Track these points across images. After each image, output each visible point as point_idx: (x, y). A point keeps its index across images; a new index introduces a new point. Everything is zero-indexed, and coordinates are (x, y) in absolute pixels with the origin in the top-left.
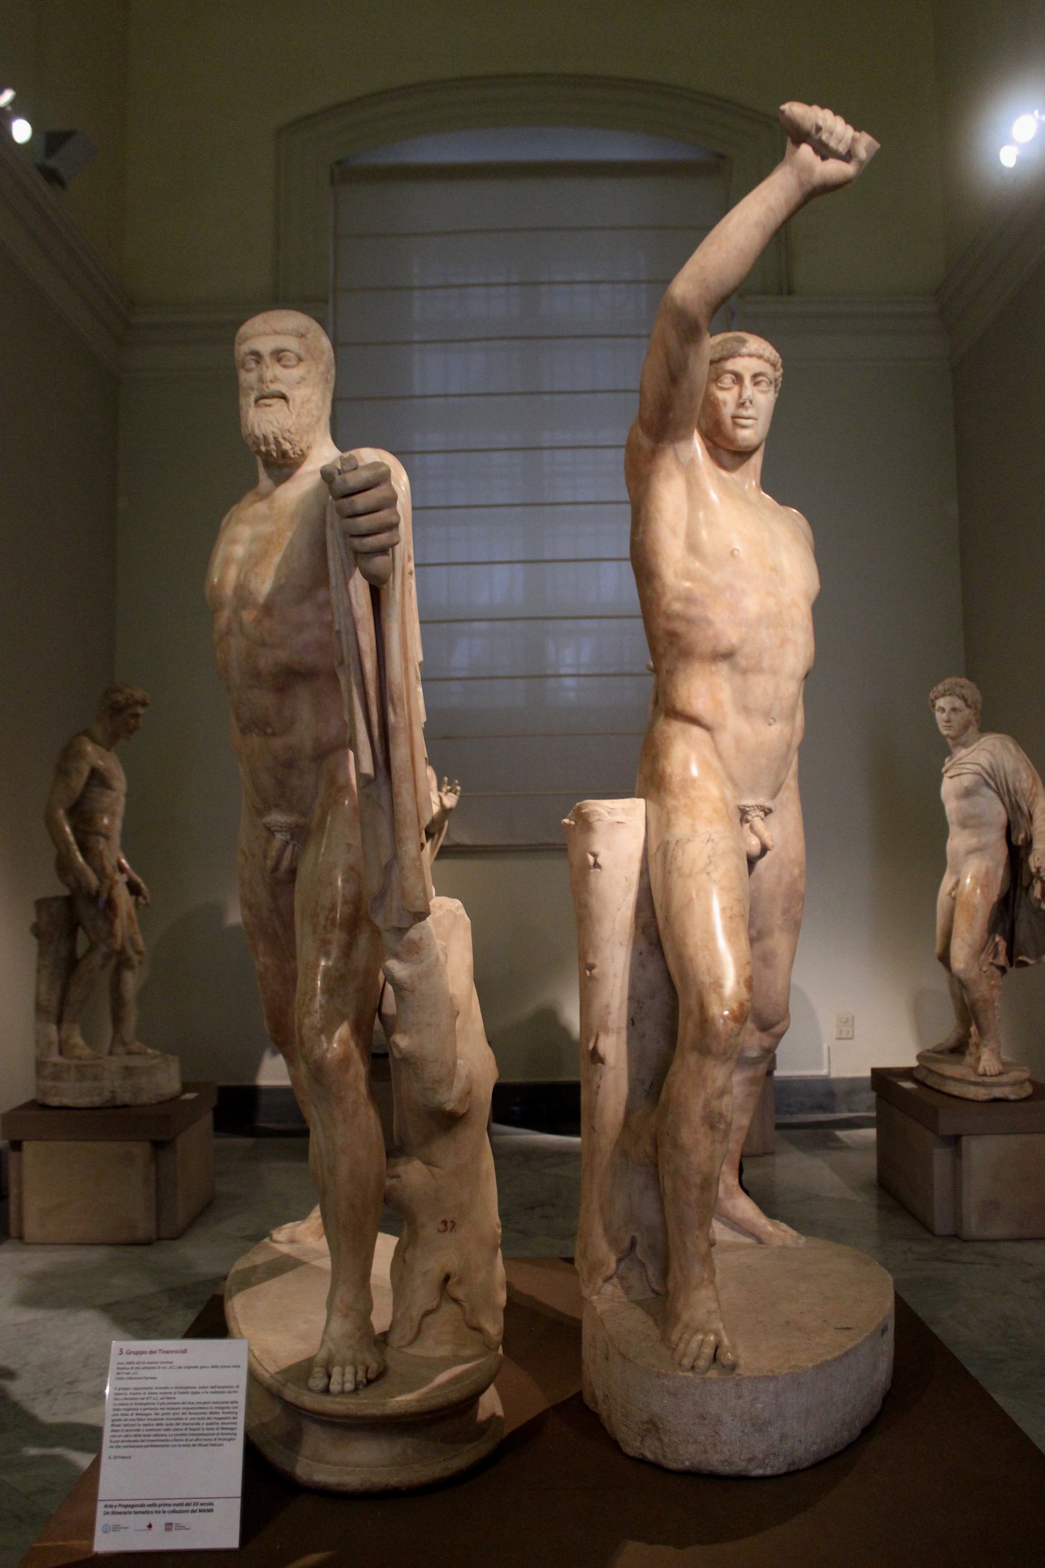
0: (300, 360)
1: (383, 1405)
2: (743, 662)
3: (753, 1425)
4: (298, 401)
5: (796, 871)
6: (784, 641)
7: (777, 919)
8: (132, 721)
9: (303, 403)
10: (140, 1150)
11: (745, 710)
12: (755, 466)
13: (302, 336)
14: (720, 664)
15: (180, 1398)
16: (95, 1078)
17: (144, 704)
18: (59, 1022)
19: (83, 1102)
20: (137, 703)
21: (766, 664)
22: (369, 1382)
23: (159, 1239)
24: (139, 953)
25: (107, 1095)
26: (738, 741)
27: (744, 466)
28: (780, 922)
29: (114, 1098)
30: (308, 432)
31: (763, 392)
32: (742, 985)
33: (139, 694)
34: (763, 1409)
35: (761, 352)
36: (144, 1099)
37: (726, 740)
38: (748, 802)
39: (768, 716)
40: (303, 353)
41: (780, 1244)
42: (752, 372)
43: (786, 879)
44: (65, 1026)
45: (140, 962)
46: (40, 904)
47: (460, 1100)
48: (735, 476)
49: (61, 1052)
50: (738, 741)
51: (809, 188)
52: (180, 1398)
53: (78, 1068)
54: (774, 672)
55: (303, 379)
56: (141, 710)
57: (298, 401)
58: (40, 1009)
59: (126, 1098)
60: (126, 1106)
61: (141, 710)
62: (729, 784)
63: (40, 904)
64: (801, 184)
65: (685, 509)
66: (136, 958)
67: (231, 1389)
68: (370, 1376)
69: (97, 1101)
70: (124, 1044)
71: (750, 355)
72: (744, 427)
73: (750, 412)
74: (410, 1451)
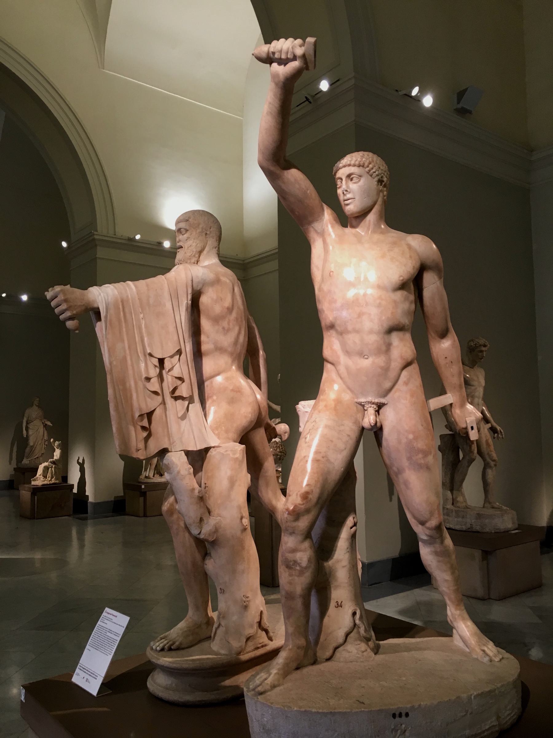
0: (187, 231)
1: (159, 659)
2: (339, 329)
3: (263, 729)
4: (186, 248)
5: (411, 436)
6: (360, 315)
7: (405, 463)
8: (480, 354)
9: (188, 247)
10: (478, 554)
11: (348, 353)
12: (370, 221)
13: (187, 220)
14: (331, 331)
15: (108, 634)
16: (463, 517)
17: (485, 346)
18: (452, 490)
19: (458, 527)
20: (480, 345)
21: (350, 328)
22: (170, 649)
23: (490, 599)
24: (494, 461)
25: (469, 526)
26: (347, 368)
27: (362, 224)
28: (407, 464)
29: (472, 527)
30: (190, 259)
31: (355, 183)
32: (299, 496)
33: (482, 341)
34: (267, 721)
35: (349, 163)
36: (487, 530)
37: (342, 369)
38: (362, 400)
39: (362, 355)
40: (187, 228)
41: (476, 657)
42: (346, 175)
43: (404, 441)
44: (455, 492)
45: (495, 465)
46: (442, 437)
47: (209, 535)
48: (357, 230)
49: (453, 504)
50: (347, 368)
51: (281, 84)
52: (108, 634)
53: (456, 511)
54: (357, 331)
55: (188, 238)
56: (483, 349)
57: (186, 248)
58: (443, 484)
59: (478, 528)
60: (478, 532)
61: (483, 349)
62: (349, 392)
63: (442, 437)
64: (277, 84)
65: (323, 254)
66: (492, 463)
67: (116, 634)
68: (172, 647)
69: (464, 528)
70: (490, 503)
71: (344, 166)
72: (347, 205)
73: (349, 196)
74: (174, 685)
